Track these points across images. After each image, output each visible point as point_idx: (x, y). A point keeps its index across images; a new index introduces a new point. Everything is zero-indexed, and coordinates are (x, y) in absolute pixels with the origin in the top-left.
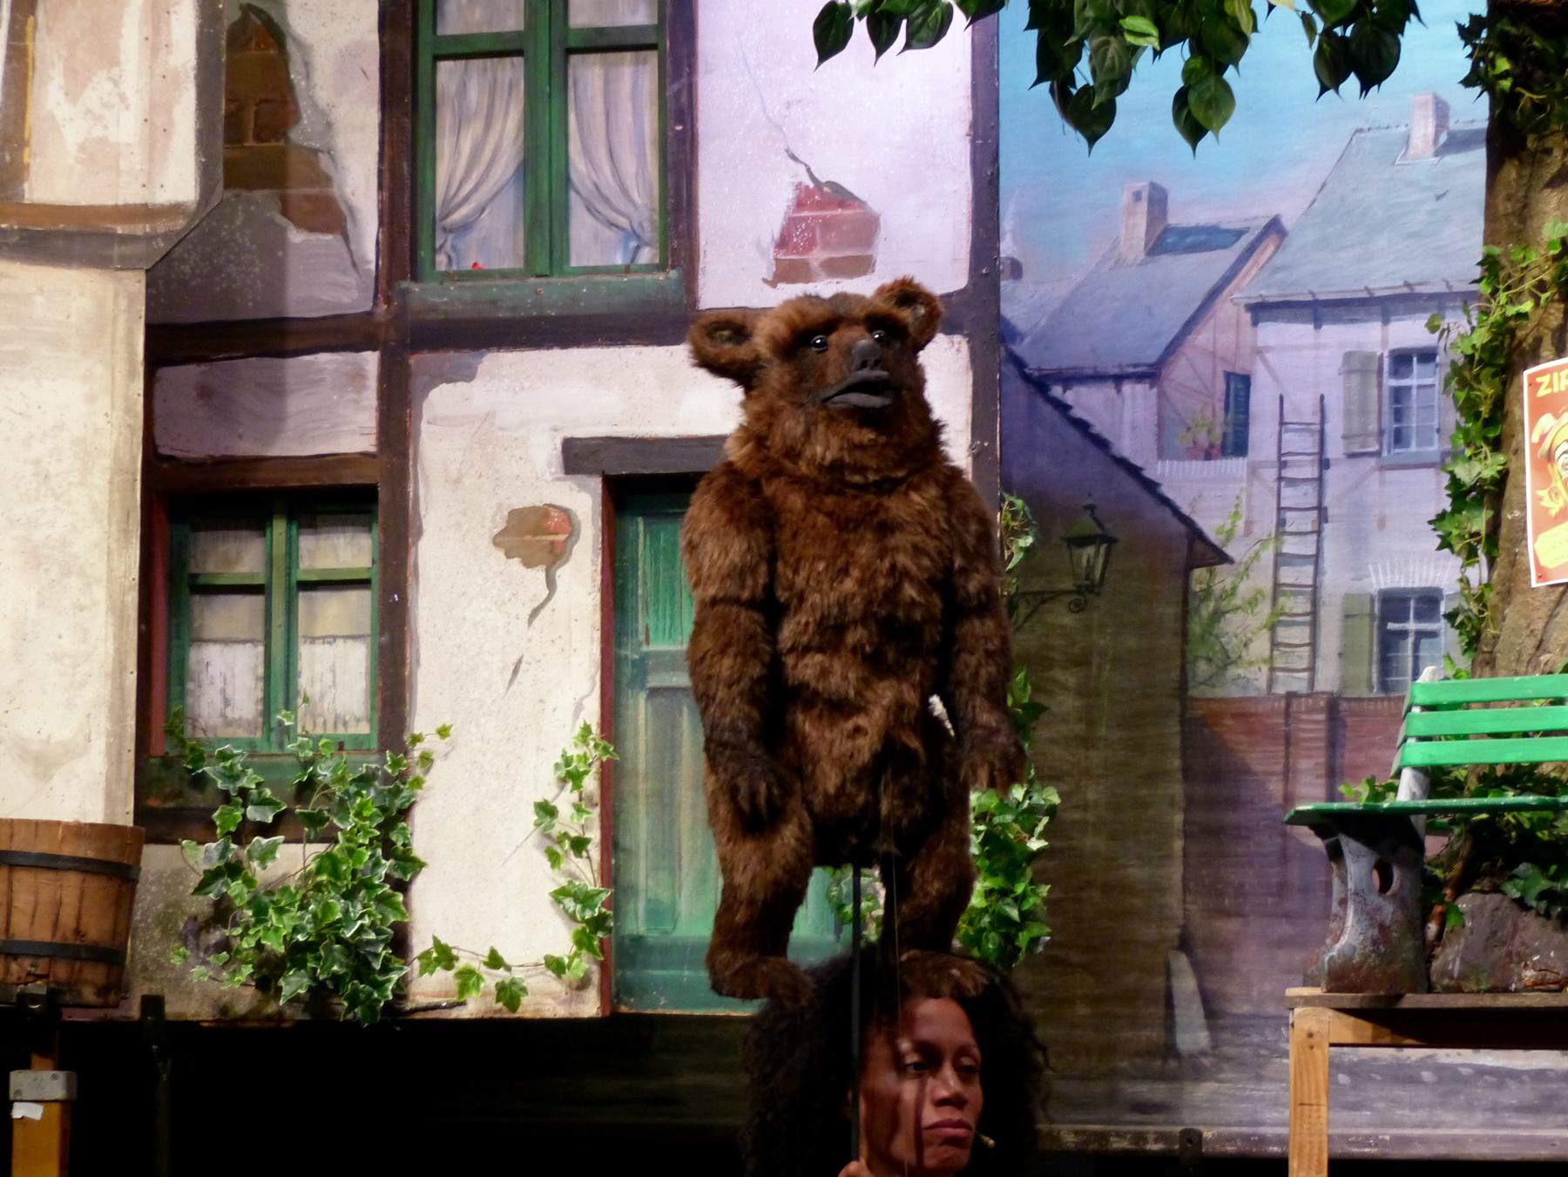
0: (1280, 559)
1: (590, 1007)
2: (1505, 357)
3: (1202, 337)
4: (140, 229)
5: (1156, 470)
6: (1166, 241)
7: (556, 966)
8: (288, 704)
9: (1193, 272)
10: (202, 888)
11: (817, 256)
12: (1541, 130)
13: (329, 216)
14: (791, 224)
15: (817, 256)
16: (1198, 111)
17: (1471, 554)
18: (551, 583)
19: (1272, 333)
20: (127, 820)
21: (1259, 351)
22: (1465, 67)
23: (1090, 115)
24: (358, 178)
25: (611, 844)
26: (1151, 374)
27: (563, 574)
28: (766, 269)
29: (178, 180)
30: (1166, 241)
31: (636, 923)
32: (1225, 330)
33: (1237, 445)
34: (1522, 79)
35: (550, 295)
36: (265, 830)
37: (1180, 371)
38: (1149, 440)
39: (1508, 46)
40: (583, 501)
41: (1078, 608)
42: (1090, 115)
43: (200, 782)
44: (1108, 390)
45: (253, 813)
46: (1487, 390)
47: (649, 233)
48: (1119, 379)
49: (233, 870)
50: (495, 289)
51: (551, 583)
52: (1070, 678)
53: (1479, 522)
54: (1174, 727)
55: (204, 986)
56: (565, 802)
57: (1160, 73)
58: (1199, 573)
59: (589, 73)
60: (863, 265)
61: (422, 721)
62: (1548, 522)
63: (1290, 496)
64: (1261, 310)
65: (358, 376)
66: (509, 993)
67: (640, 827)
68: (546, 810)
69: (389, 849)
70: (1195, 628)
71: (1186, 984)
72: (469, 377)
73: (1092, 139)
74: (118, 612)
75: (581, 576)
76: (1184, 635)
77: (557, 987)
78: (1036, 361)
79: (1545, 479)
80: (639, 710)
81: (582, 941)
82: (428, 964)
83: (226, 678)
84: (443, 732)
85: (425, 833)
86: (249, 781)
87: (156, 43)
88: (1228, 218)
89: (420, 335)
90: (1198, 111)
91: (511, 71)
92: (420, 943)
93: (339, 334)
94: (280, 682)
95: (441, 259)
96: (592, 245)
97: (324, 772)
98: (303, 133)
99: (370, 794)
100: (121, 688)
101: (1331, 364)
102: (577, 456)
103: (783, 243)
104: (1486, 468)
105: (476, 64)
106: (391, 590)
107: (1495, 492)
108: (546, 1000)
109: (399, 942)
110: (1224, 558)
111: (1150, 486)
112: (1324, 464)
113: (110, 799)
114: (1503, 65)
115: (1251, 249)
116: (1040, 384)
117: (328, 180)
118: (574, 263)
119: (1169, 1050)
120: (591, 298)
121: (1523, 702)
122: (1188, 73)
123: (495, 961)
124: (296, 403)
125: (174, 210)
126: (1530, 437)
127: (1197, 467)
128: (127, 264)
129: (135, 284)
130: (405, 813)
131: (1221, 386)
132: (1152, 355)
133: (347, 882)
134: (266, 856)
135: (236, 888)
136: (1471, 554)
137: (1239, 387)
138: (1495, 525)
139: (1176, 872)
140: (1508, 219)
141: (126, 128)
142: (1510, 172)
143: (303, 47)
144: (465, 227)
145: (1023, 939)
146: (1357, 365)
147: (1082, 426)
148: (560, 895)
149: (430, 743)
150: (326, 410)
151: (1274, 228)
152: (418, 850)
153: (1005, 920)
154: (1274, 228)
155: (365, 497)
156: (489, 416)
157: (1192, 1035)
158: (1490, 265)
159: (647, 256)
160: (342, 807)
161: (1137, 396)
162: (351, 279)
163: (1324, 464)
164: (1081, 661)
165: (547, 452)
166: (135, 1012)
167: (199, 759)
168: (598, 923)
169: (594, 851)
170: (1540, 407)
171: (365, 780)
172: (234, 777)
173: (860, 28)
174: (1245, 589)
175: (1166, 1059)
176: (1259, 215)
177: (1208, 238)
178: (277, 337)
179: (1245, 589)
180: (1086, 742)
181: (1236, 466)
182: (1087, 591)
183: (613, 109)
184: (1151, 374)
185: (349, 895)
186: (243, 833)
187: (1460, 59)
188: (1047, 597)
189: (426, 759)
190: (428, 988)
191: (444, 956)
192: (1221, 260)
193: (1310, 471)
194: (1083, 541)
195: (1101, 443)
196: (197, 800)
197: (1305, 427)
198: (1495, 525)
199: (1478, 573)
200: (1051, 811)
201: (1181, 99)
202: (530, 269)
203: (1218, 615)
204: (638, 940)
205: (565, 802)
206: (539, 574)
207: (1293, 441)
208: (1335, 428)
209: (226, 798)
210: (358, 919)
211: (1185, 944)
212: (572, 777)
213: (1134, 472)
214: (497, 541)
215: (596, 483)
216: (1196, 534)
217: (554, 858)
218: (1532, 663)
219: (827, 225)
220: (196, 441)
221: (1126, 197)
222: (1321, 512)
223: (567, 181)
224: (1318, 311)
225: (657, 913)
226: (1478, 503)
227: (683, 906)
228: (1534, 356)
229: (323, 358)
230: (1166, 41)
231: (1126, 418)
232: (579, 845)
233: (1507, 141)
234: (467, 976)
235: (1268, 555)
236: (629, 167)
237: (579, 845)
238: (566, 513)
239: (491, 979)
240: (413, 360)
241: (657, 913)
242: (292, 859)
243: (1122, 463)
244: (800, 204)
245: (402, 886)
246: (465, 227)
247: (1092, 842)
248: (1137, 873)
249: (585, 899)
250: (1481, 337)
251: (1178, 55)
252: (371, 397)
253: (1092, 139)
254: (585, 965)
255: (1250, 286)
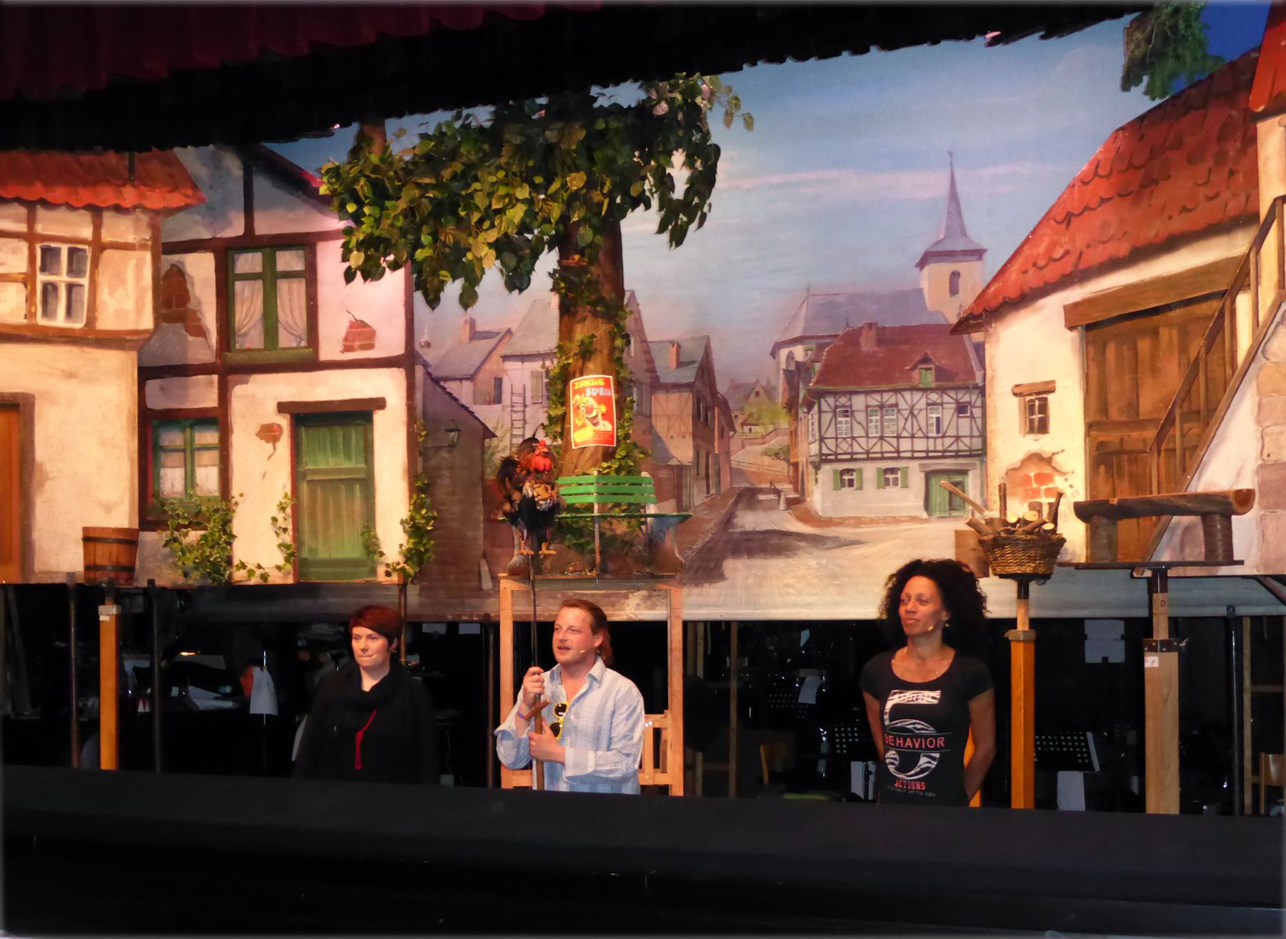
0: (512, 436)
1: (290, 581)
2: (566, 375)
3: (487, 366)
4: (135, 337)
5: (474, 408)
6: (475, 335)
7: (279, 568)
8: (193, 487)
9: (485, 345)
10: (165, 545)
11: (356, 344)
12: (575, 306)
13: (200, 332)
14: (348, 333)
15: (356, 344)
16: (468, 299)
17: (555, 438)
18: (275, 448)
19: (510, 365)
20: (136, 526)
21: (505, 371)
22: (550, 286)
23: (433, 301)
24: (210, 318)
25: (296, 529)
26: (471, 378)
27: (279, 445)
28: (340, 347)
29: (147, 321)
30: (475, 335)
31: (305, 555)
32: (494, 365)
33: (498, 399)
34: (568, 289)
35: (271, 357)
36: (186, 527)
37: (480, 377)
38: (471, 397)
39: (563, 279)
40: (284, 422)
41: (449, 452)
42: (433, 301)
43: (165, 512)
44: (458, 383)
45: (181, 521)
46: (559, 386)
47: (304, 337)
48: (461, 380)
49: (175, 540)
50: (254, 355)
51: (275, 448)
52: (447, 473)
53: (558, 429)
54: (480, 489)
55: (167, 577)
56: (280, 517)
57: (453, 289)
58: (487, 441)
59: (283, 285)
60: (370, 347)
61: (235, 492)
62: (577, 428)
63: (515, 416)
64: (506, 358)
65: (211, 383)
66: (264, 577)
67: (306, 525)
68: (275, 520)
69: (225, 532)
70: (486, 457)
71: (485, 569)
72: (247, 383)
73: (433, 309)
74: (131, 460)
75: (284, 445)
76: (483, 460)
77: (280, 574)
78: (436, 374)
79: (576, 414)
80: (304, 487)
81: (287, 560)
82: (238, 568)
83: (172, 479)
84: (241, 495)
85: (237, 526)
86: (180, 512)
87: (138, 277)
88: (494, 329)
89: (231, 368)
90: (468, 299)
91: (259, 285)
92: (236, 562)
93: (205, 369)
94: (190, 480)
95: (238, 346)
96: (286, 340)
97: (204, 508)
98: (192, 305)
99: (217, 515)
100: (132, 483)
101: (527, 375)
102: (282, 407)
103: (346, 339)
104: (560, 411)
105: (247, 283)
106: (224, 449)
107: (563, 419)
108: (276, 578)
109: (229, 561)
110: (495, 436)
111: (472, 413)
112: (525, 406)
113: (131, 520)
114: (563, 285)
115: (502, 338)
116: (436, 381)
117: (199, 320)
118: (281, 345)
119: (480, 589)
120: (285, 357)
121: (570, 485)
122: (464, 288)
123: (259, 567)
124: (192, 391)
125: (146, 331)
126: (572, 402)
127: (486, 407)
128: (131, 349)
129: (133, 355)
130: (230, 521)
131: (493, 382)
132: (472, 372)
133: (211, 543)
134: (186, 535)
135: (176, 545)
136: (555, 438)
137: (499, 381)
138: (563, 428)
139: (481, 533)
140: (566, 332)
141: (129, 305)
142: (566, 318)
143: (191, 278)
144: (245, 335)
145: (426, 557)
146: (535, 375)
147: (450, 394)
148: (280, 546)
149: (237, 498)
150: (203, 394)
151: (509, 332)
152: (235, 532)
153: (419, 552)
154: (509, 332)
155: (218, 419)
156: (253, 396)
157: (487, 584)
158: (559, 347)
159: (303, 344)
160: (209, 522)
161: (467, 385)
162: (208, 352)
163: (525, 406)
164: (451, 468)
165: (272, 407)
166: (145, 585)
167: (163, 505)
168: (292, 555)
169: (290, 532)
170: (576, 392)
171: (216, 511)
172: (174, 510)
173: (359, 273)
174: (501, 446)
175: (479, 592)
176: (504, 327)
177: (487, 335)
178: (185, 371)
179: (501, 446)
180: (453, 494)
181: (498, 407)
182: (452, 446)
183: (291, 296)
184: (471, 378)
185: (212, 547)
186: (179, 527)
187: (549, 283)
188: (439, 448)
189: (236, 504)
190: (239, 576)
191: (243, 566)
192: (492, 342)
193: (521, 409)
194: (451, 431)
195: (456, 400)
196: (163, 517)
197: (519, 395)
198: (563, 428)
199: (559, 442)
200: (434, 518)
201: (461, 296)
202: (266, 349)
203: (493, 454)
204: (306, 559)
205: (280, 517)
206: (270, 446)
207: (516, 399)
208: (528, 395)
209: (172, 517)
210: (215, 555)
211: (484, 556)
212: (283, 509)
213: (466, 409)
214: (258, 435)
215: (288, 416)
216: (486, 428)
217: (277, 534)
218: (573, 473)
219: (360, 334)
220: (157, 402)
221: (462, 322)
222: (524, 420)
223: (277, 320)
224: (523, 358)
225: (311, 551)
226: (556, 423)
227: (320, 547)
228: (574, 377)
229: (200, 377)
230: (454, 278)
231: (464, 392)
232: (285, 530)
233: (567, 309)
234: (251, 573)
235: (508, 435)
236: (297, 315)
237: (285, 530)
238: (279, 426)
239: (259, 572)
240: (230, 378)
241: (311, 551)
242: (194, 536)
243: (463, 406)
244: (351, 327)
245: (230, 544)
246: (245, 335)
247: (455, 525)
248: (470, 534)
249: (287, 547)
250: (557, 371)
251: (460, 282)
252: (216, 390)
253: (433, 309)
254: (289, 567)
255: (503, 350)
